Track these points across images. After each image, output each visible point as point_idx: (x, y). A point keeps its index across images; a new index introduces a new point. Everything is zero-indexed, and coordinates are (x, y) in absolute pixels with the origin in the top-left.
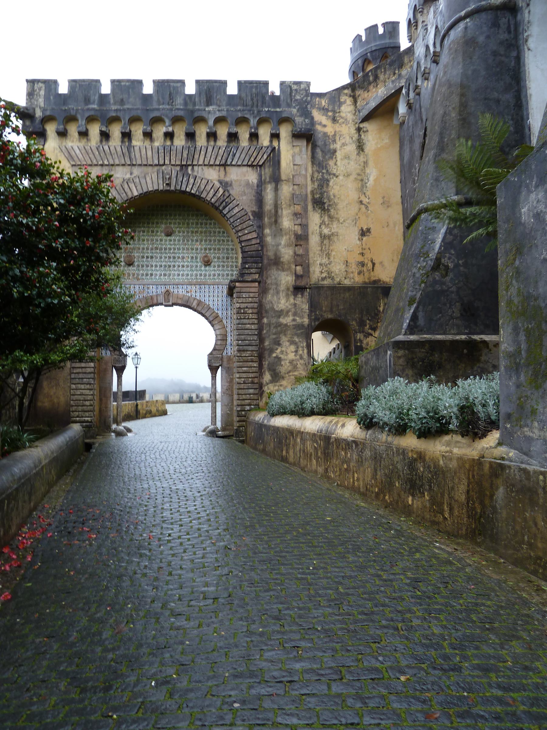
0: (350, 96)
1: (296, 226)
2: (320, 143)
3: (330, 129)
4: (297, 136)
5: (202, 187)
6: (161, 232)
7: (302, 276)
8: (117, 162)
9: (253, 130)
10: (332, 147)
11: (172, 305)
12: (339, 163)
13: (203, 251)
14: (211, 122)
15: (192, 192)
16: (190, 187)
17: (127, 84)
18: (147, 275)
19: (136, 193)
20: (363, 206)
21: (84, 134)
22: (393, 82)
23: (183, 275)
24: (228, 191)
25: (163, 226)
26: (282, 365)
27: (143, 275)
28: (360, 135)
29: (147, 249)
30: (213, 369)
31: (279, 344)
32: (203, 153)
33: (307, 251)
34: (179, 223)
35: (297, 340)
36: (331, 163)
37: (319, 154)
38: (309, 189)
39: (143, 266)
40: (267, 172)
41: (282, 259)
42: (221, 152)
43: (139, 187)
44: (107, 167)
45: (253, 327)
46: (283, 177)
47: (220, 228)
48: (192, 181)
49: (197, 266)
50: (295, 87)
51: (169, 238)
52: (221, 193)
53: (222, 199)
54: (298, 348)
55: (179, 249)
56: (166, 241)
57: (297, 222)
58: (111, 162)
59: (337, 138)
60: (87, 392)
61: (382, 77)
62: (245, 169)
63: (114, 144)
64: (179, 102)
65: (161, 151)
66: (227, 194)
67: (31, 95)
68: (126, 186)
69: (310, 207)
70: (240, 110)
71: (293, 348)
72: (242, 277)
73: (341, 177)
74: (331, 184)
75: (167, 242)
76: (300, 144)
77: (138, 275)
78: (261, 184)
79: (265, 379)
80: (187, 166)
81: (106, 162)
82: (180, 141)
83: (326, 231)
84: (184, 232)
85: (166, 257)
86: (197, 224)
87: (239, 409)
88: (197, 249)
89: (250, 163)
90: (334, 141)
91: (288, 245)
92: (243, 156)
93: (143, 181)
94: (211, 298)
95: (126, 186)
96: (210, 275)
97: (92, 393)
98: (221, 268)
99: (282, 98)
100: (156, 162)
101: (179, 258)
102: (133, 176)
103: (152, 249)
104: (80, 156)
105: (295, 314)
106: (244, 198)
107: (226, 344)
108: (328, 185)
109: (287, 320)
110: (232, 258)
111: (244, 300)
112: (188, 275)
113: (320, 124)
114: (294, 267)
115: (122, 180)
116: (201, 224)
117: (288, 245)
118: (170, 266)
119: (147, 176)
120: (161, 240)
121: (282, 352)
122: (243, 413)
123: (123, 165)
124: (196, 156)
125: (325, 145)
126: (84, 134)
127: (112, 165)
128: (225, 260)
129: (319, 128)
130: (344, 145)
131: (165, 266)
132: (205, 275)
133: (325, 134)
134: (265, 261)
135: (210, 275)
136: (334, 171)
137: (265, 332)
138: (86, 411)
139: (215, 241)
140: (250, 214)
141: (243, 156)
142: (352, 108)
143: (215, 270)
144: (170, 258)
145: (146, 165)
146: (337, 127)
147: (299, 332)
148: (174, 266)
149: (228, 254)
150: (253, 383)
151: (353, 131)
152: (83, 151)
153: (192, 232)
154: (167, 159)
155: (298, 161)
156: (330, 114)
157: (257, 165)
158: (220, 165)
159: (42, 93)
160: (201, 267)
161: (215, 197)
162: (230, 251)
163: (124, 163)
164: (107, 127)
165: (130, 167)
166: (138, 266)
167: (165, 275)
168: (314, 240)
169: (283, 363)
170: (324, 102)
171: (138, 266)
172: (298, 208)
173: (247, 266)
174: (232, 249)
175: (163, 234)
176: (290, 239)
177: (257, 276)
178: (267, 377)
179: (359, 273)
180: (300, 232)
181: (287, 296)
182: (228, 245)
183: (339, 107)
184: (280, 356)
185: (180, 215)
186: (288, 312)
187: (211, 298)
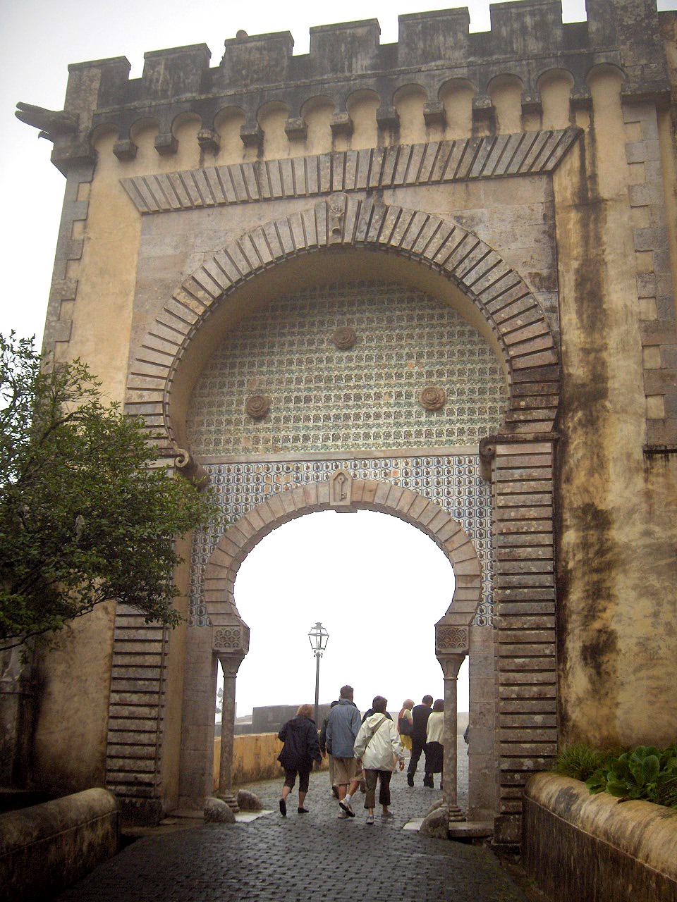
1: (643, 302)
4: (631, 102)
5: (415, 230)
6: (331, 342)
8: (231, 198)
9: (528, 99)
11: (353, 507)
13: (423, 380)
14: (432, 94)
15: (393, 243)
16: (387, 232)
17: (259, 44)
18: (296, 439)
19: (267, 258)
23: (377, 436)
24: (475, 235)
25: (335, 328)
26: (618, 652)
27: (286, 439)
29: (299, 381)
30: (449, 662)
31: (610, 597)
32: (416, 159)
34: (370, 320)
35: (658, 585)
39: (287, 420)
40: (566, 184)
41: (610, 384)
42: (457, 153)
43: (275, 245)
44: (210, 211)
45: (540, 552)
47: (462, 324)
48: (391, 219)
49: (409, 414)
51: (346, 354)
52: (458, 240)
53: (462, 252)
54: (659, 604)
55: (369, 377)
56: (340, 360)
57: (644, 293)
58: (220, 198)
60: (145, 711)
62: (512, 183)
63: (228, 164)
64: (362, 63)
65: (326, 164)
66: (471, 241)
67: (74, 91)
68: (247, 245)
70: (498, 62)
71: (646, 605)
72: (513, 429)
75: (341, 362)
76: (640, 118)
77: (276, 440)
79: (573, 689)
80: (380, 190)
81: (209, 201)
82: (366, 140)
84: (380, 339)
85: (339, 398)
86: (411, 318)
87: (505, 766)
88: (410, 375)
89: (524, 169)
91: (624, 347)
92: (506, 159)
93: (284, 231)
94: (444, 488)
95: (247, 245)
96: (440, 434)
97: (154, 713)
98: (465, 417)
99: (593, 27)
100: (313, 188)
101: (368, 396)
102: (263, 223)
103: (309, 381)
104: (159, 196)
105: (650, 516)
106: (513, 246)
107: (481, 600)
110: (493, 391)
111: (518, 487)
112: (388, 435)
114: (644, 399)
115: (239, 233)
116: (421, 318)
117: (624, 347)
118: (347, 417)
119: (293, 220)
120: (329, 360)
122: (517, 776)
123: (244, 202)
126: (168, 150)
127: (222, 205)
128: (476, 396)
131: (337, 417)
132: (429, 434)
135: (440, 434)
137: (571, 565)
138: (140, 758)
139: (452, 354)
140: (527, 281)
141: (506, 159)
143: (451, 422)
144: (347, 397)
145: (291, 198)
147: (660, 563)
148: (357, 416)
149: (482, 381)
150: (540, 698)
152: (166, 184)
153: (400, 338)
154: (337, 179)
157: (542, 172)
158: (455, 181)
159: (96, 85)
160: (419, 414)
161: (444, 251)
162: (487, 377)
163: (244, 196)
164: (213, 130)
165: (257, 206)
166: (277, 420)
167: (336, 437)
169: (621, 644)
171: (277, 420)
173: (523, 403)
174: (493, 371)
175: (333, 347)
176: (628, 333)
177: (547, 426)
178: (578, 681)
180: (653, 316)
181: (630, 472)
182: (484, 361)
184: (613, 626)
185: (371, 302)
186: (631, 512)
187: (444, 488)
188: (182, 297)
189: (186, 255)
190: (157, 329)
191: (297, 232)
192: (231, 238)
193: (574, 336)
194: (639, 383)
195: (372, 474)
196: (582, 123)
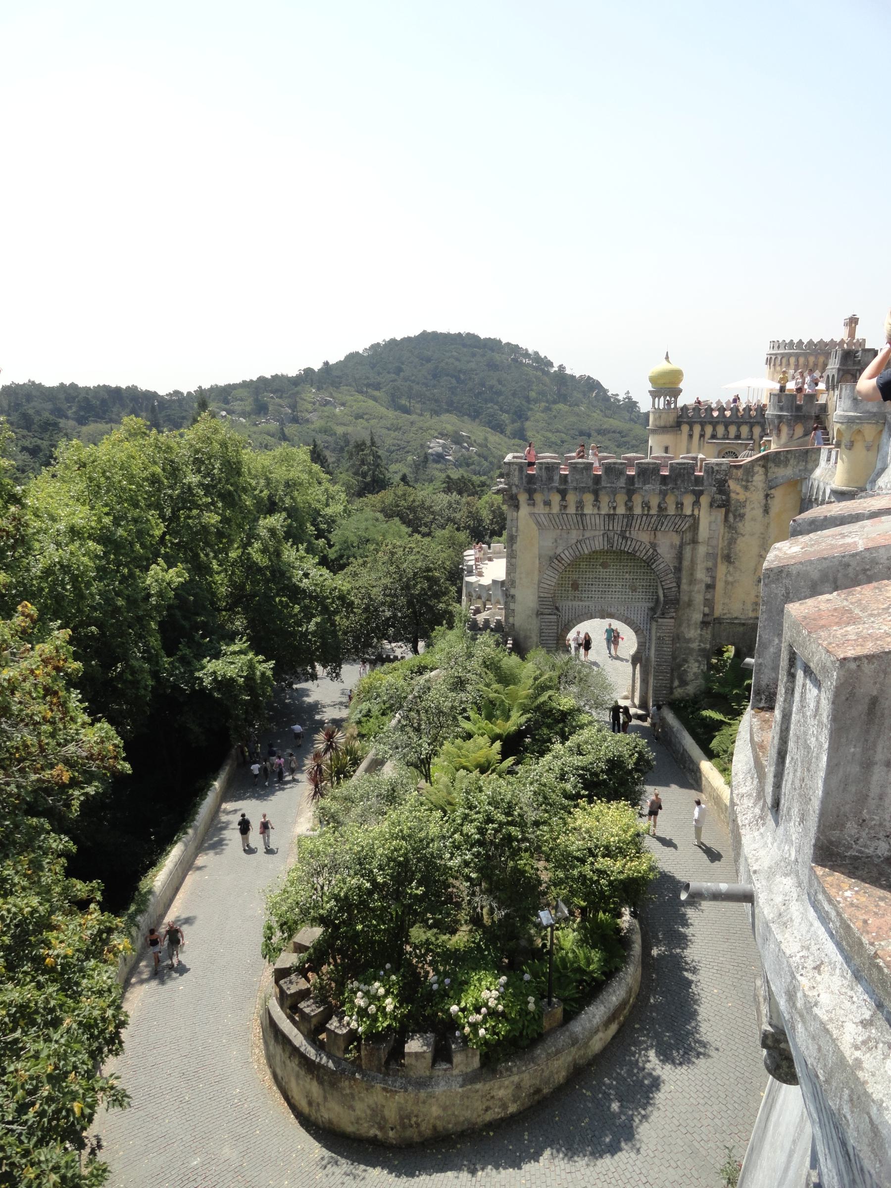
0: (763, 466)
2: (732, 508)
3: (741, 497)
5: (637, 548)
7: (708, 615)
10: (742, 511)
21: (547, 503)
22: (800, 471)
32: (639, 521)
33: (714, 596)
36: (740, 525)
37: (731, 518)
38: (720, 546)
40: (688, 536)
42: (653, 520)
46: (700, 540)
48: (629, 543)
50: (716, 468)
59: (748, 503)
61: (792, 461)
64: (622, 482)
68: (579, 546)
69: (719, 560)
71: (697, 664)
73: (747, 536)
74: (738, 541)
78: (681, 546)
80: (626, 531)
83: (730, 579)
90: (744, 506)
92: (670, 524)
93: (592, 542)
95: (579, 546)
99: (705, 478)
104: (546, 523)
105: (700, 641)
109: (695, 645)
121: (688, 667)
124: (633, 524)
126: (547, 503)
129: (733, 495)
130: (753, 509)
133: (738, 501)
134: (681, 603)
136: (742, 532)
141: (670, 524)
142: (762, 477)
146: (748, 494)
155: (714, 527)
156: (744, 483)
159: (517, 473)
168: (720, 585)
170: (740, 473)
172: (710, 564)
178: (676, 683)
179: (753, 610)
181: (696, 628)
183: (752, 476)
188: (556, 562)
189: (557, 547)
190: (547, 572)
191: (597, 543)
193: (684, 587)
194: (702, 602)
195: (613, 610)
196: (696, 512)
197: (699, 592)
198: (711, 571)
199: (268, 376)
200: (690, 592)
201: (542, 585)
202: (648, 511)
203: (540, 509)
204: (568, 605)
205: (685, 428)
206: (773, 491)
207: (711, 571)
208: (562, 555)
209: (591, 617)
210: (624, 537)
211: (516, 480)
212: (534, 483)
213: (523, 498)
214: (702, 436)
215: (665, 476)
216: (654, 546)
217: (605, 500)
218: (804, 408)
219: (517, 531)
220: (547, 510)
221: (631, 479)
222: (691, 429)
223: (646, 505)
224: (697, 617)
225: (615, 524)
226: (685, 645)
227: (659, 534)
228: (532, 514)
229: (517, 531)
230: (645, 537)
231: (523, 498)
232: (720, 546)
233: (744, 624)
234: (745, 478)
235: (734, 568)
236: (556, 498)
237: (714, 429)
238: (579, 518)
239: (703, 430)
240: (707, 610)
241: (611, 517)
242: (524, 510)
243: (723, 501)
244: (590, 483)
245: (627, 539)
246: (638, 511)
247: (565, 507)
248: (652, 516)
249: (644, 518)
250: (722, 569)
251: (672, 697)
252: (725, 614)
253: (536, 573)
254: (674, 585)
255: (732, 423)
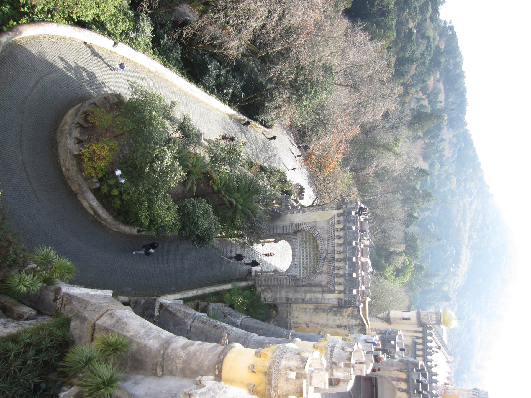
0: (359, 324)
2: (339, 310)
3: (344, 314)
10: (338, 314)
12: (332, 317)
20: (316, 325)
21: (339, 223)
24: (319, 274)
28: (343, 326)
30: (273, 272)
32: (332, 265)
36: (332, 314)
40: (325, 289)
42: (332, 271)
46: (324, 295)
48: (322, 261)
59: (342, 317)
64: (348, 255)
71: (270, 296)
74: (324, 313)
78: (321, 286)
80: (327, 259)
83: (307, 310)
92: (330, 279)
93: (322, 244)
105: (280, 298)
108: (324, 312)
109: (278, 295)
113: (347, 310)
115: (323, 237)
117: (301, 295)
124: (330, 263)
125: (338, 312)
129: (345, 310)
130: (339, 320)
133: (343, 312)
141: (330, 279)
142: (354, 323)
146: (346, 317)
151: (345, 323)
159: (352, 206)
168: (304, 306)
172: (313, 300)
178: (263, 288)
179: (294, 322)
183: (354, 319)
192: (322, 236)
193: (303, 289)
196: (336, 292)
197: (301, 295)
198: (310, 301)
199: (481, 167)
200: (301, 292)
201: (304, 224)
202: (337, 269)
203: (336, 219)
204: (298, 238)
205: (421, 329)
206: (348, 329)
207: (310, 301)
208: (316, 232)
209: (292, 250)
210: (324, 259)
211: (349, 206)
212: (347, 215)
213: (341, 211)
214: (417, 338)
215: (352, 275)
216: (321, 273)
217: (341, 249)
218: (389, 344)
219: (327, 210)
220: (336, 222)
221: (350, 259)
222: (420, 332)
223: (339, 268)
224: (290, 296)
225: (330, 254)
226: (278, 290)
227: (326, 275)
228: (334, 216)
229: (327, 210)
230: (325, 268)
231: (341, 211)
232: (322, 305)
233: (287, 317)
234: (354, 315)
235: (312, 312)
236: (341, 226)
237: (420, 344)
238: (332, 237)
239: (420, 338)
240: (293, 300)
241: (333, 252)
242: (336, 212)
243: (341, 304)
244: (349, 240)
245: (324, 260)
246: (337, 264)
247: (338, 231)
248: (335, 271)
249: (333, 267)
250: (312, 306)
251: (258, 287)
252: (292, 308)
253: (309, 221)
254: (304, 284)
255: (424, 352)
